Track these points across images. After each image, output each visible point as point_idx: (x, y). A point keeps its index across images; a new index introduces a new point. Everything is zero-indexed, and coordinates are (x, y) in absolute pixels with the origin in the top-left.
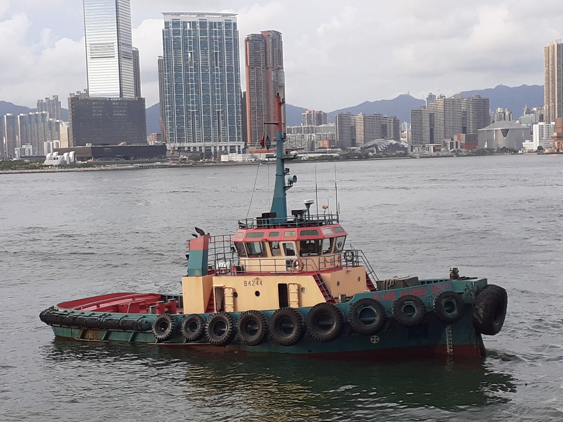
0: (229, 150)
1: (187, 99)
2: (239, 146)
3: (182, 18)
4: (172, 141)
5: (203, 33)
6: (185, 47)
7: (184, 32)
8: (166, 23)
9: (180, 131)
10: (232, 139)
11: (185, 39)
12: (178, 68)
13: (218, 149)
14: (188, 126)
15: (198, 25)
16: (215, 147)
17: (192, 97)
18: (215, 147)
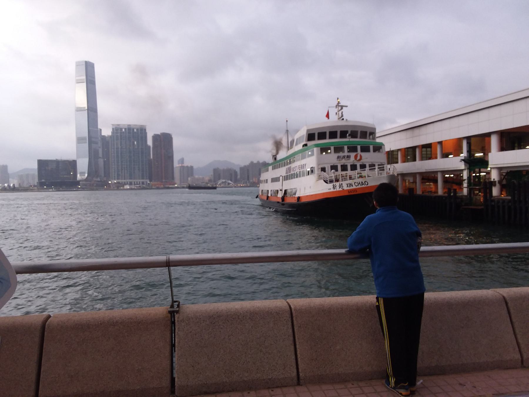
0: (141, 183)
1: (122, 162)
2: (146, 182)
3: (121, 126)
4: (115, 179)
5: (129, 133)
6: (121, 139)
7: (121, 133)
8: (113, 129)
9: (118, 175)
10: (143, 179)
11: (121, 136)
12: (117, 148)
13: (136, 183)
14: (122, 173)
15: (127, 130)
16: (134, 182)
17: (124, 160)
18: (134, 182)
